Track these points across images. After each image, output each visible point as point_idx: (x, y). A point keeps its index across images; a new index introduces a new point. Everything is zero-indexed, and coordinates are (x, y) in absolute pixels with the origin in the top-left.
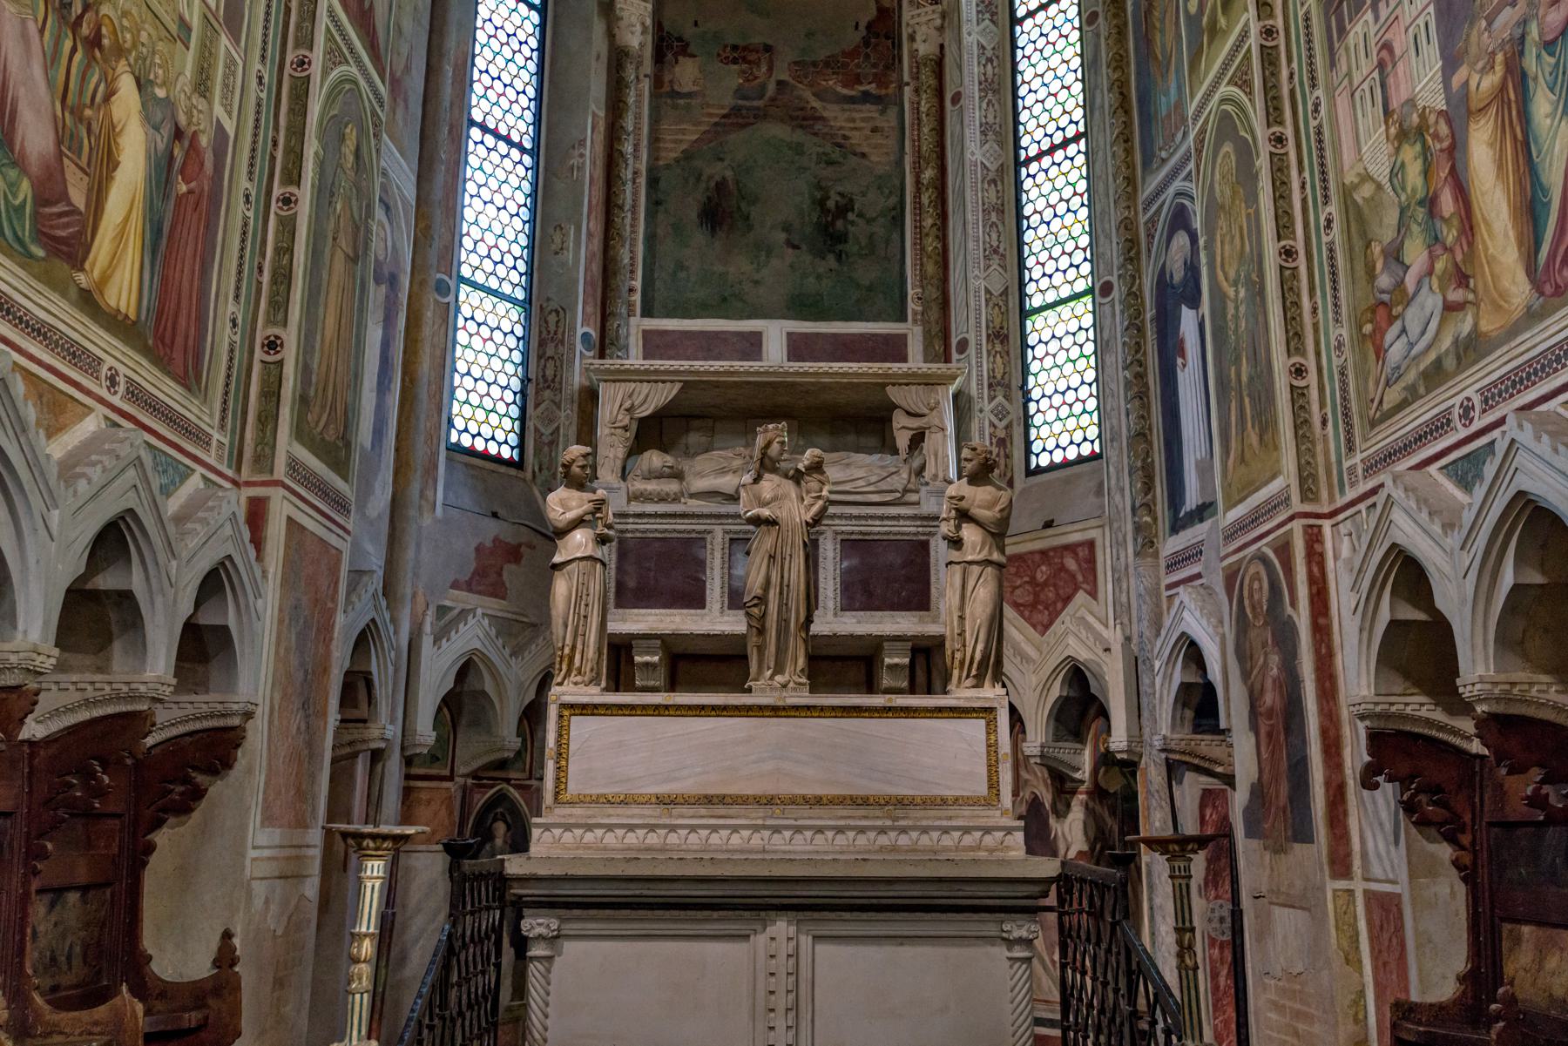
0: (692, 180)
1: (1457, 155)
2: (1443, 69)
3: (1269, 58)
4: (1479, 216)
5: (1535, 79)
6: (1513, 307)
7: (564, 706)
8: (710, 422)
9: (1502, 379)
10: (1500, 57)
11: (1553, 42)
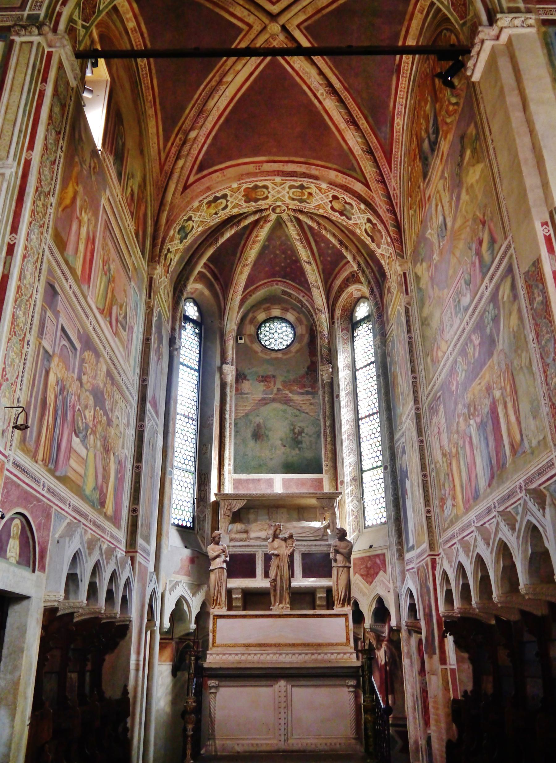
0: (248, 424)
7: (215, 616)
8: (256, 510)
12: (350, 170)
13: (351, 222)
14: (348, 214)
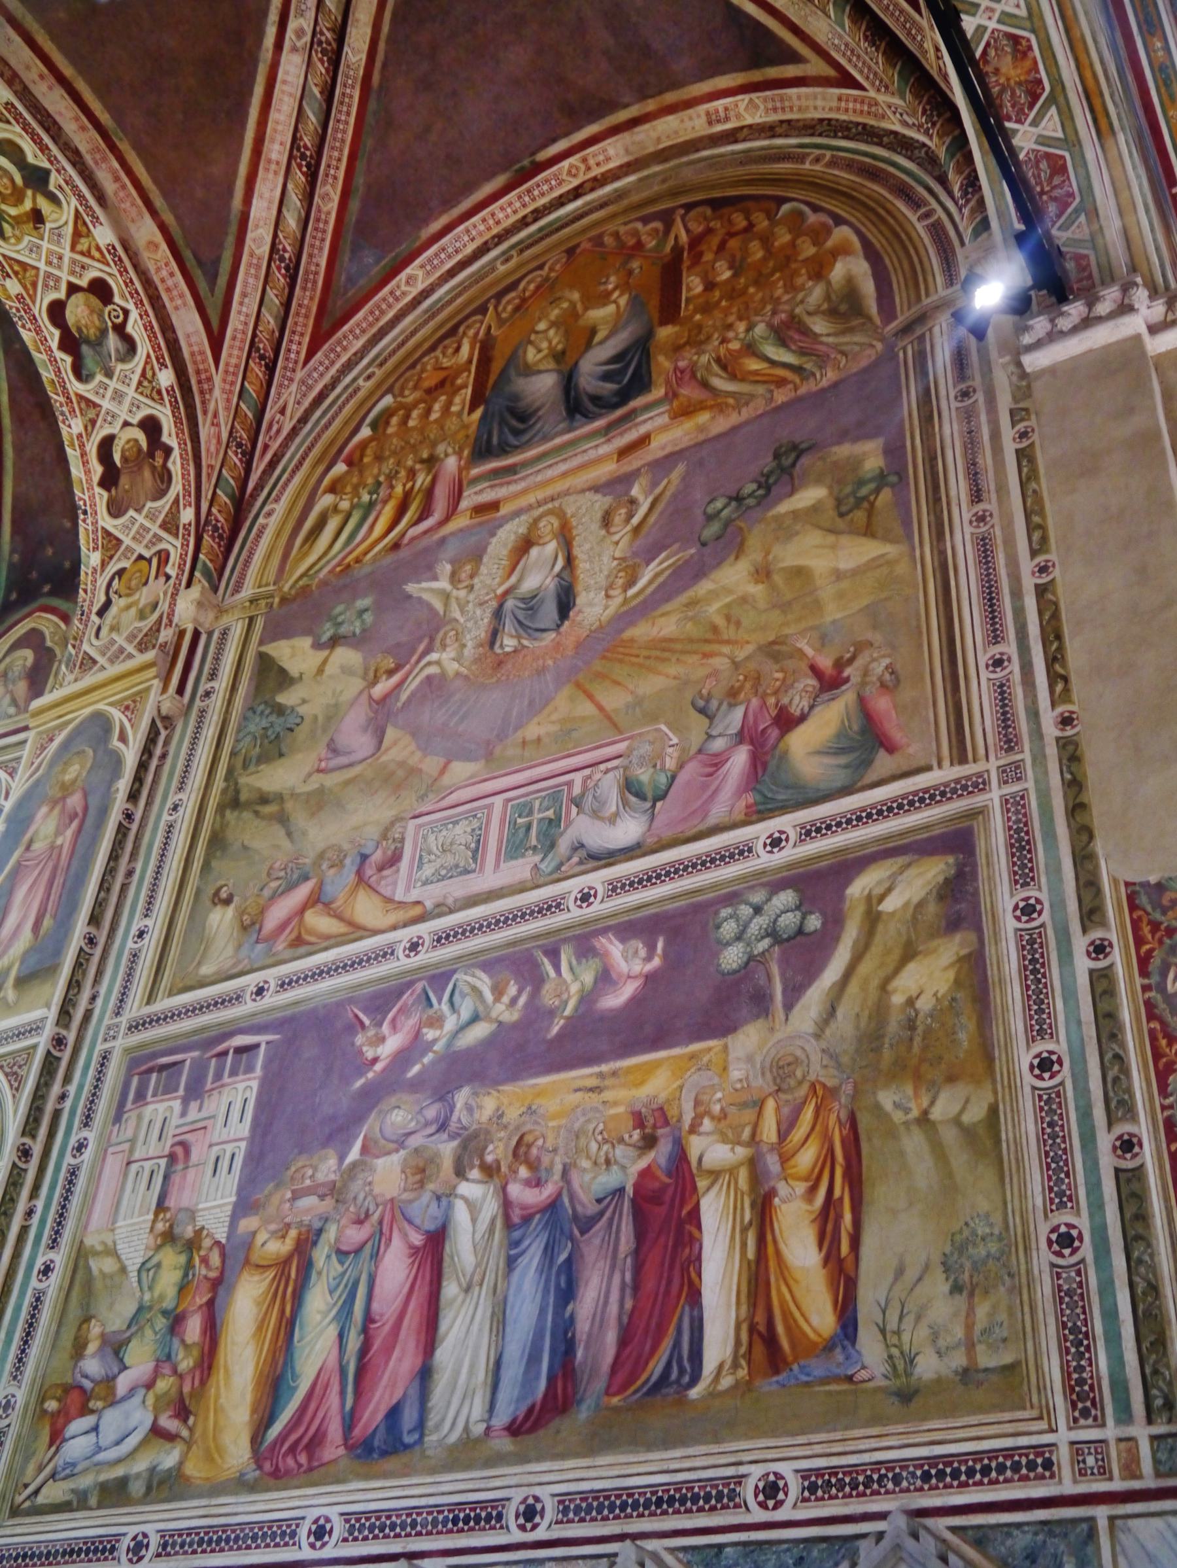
1: (221, 1291)
2: (236, 1206)
3: (49, 1065)
4: (222, 1362)
5: (319, 1273)
6: (226, 1466)
9: (189, 1531)
10: (293, 1233)
11: (347, 1253)
12: (200, 263)
13: (76, 387)
14: (89, 362)
